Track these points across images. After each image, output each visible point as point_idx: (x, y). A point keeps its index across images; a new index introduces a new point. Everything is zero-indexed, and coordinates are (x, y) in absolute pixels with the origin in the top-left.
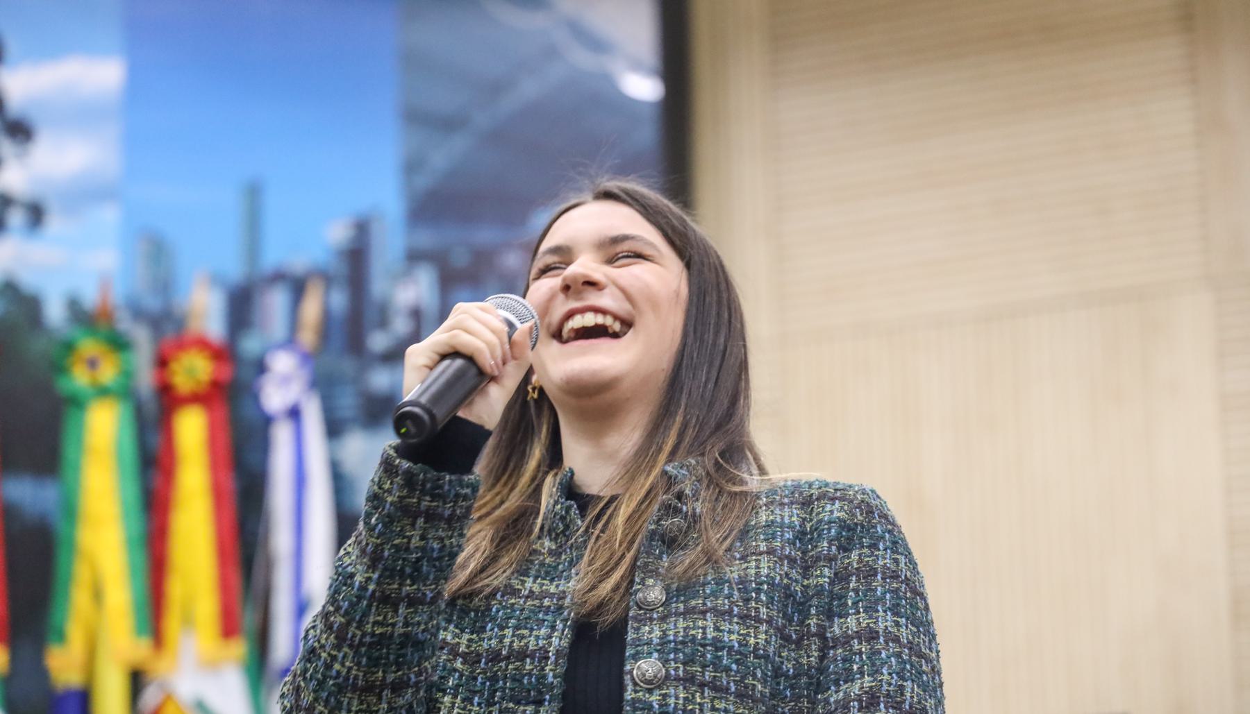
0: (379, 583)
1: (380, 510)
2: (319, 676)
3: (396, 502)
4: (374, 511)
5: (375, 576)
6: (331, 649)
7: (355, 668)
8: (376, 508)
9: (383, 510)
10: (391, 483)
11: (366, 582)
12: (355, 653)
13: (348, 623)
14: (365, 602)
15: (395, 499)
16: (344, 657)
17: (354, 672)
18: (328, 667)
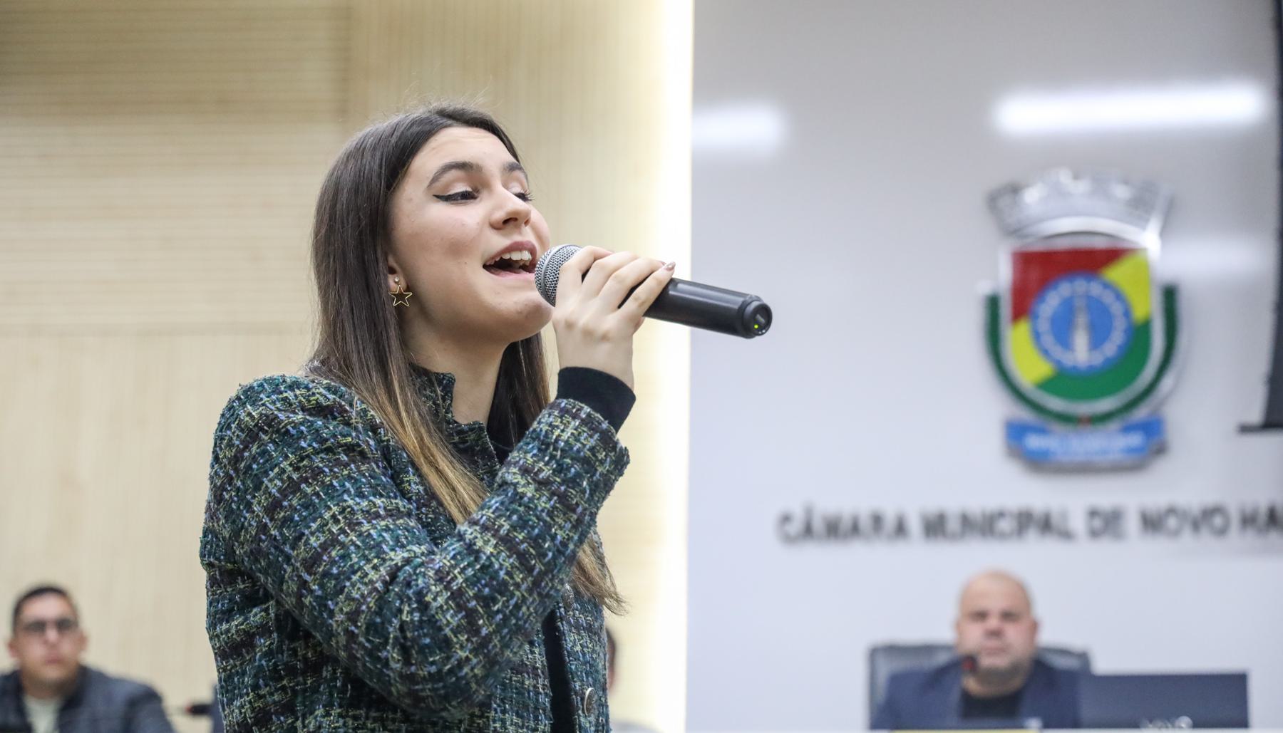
0: (575, 545)
1: (589, 475)
2: (507, 612)
3: (603, 474)
4: (584, 475)
5: (576, 537)
6: (526, 591)
7: (534, 615)
8: (587, 473)
9: (591, 477)
10: (605, 456)
11: (568, 539)
12: (540, 601)
13: (546, 573)
14: (563, 559)
15: (605, 473)
16: (533, 602)
17: (531, 618)
18: (517, 607)
